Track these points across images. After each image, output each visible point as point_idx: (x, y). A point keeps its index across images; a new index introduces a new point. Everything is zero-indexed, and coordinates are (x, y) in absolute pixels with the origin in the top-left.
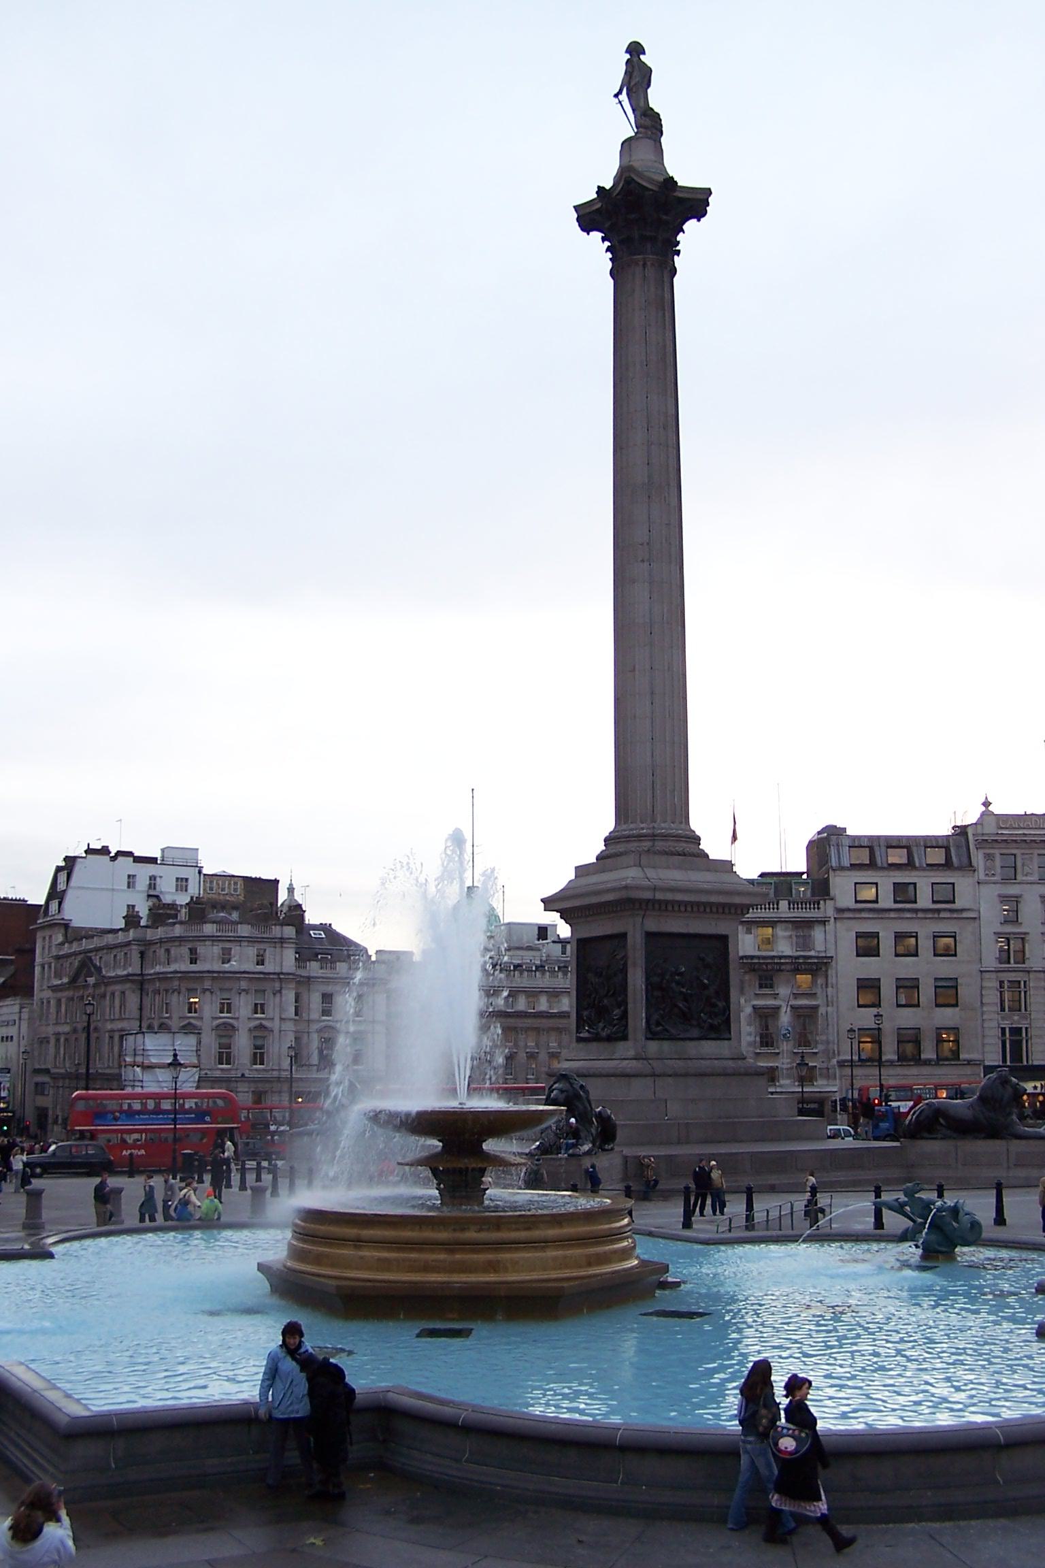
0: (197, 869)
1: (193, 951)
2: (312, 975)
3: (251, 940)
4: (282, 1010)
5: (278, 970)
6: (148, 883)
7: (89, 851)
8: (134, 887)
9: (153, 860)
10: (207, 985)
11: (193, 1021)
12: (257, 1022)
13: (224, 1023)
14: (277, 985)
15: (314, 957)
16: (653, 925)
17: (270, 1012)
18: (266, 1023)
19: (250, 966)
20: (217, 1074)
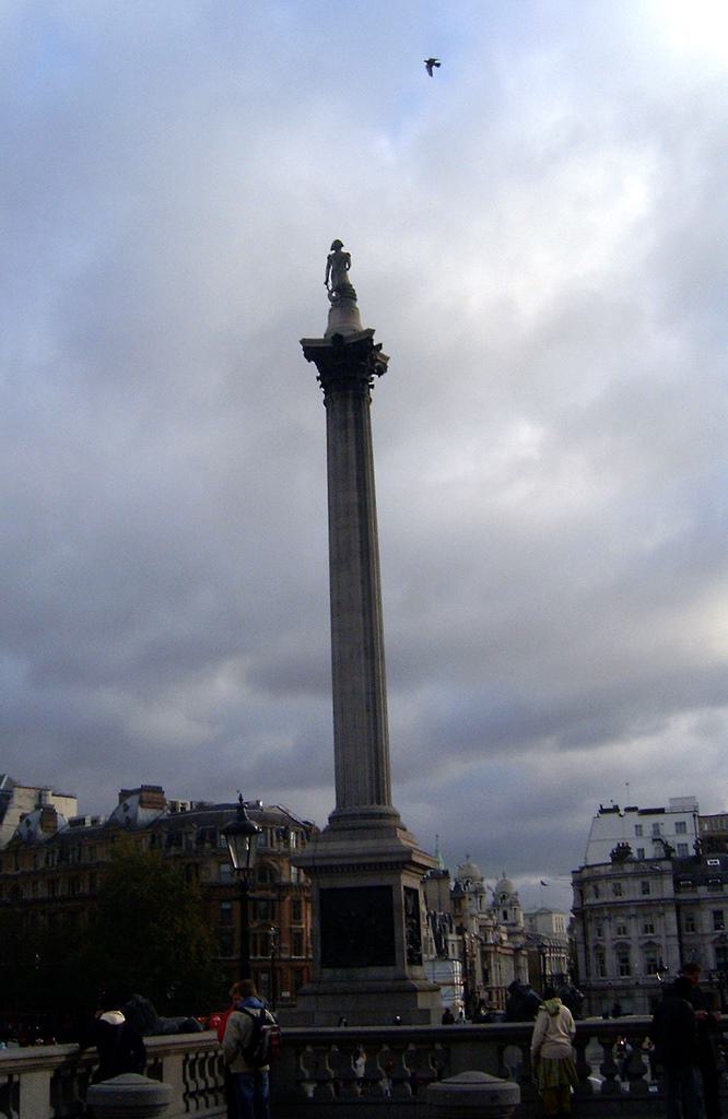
0: (691, 814)
1: (596, 888)
2: (702, 897)
3: (636, 875)
4: (666, 929)
5: (659, 896)
6: (651, 829)
7: (603, 811)
8: (641, 835)
9: (661, 811)
10: (606, 913)
11: (601, 943)
12: (647, 941)
13: (620, 943)
14: (661, 908)
15: (705, 883)
16: (326, 883)
17: (659, 930)
18: (654, 940)
19: (639, 896)
20: (619, 983)
